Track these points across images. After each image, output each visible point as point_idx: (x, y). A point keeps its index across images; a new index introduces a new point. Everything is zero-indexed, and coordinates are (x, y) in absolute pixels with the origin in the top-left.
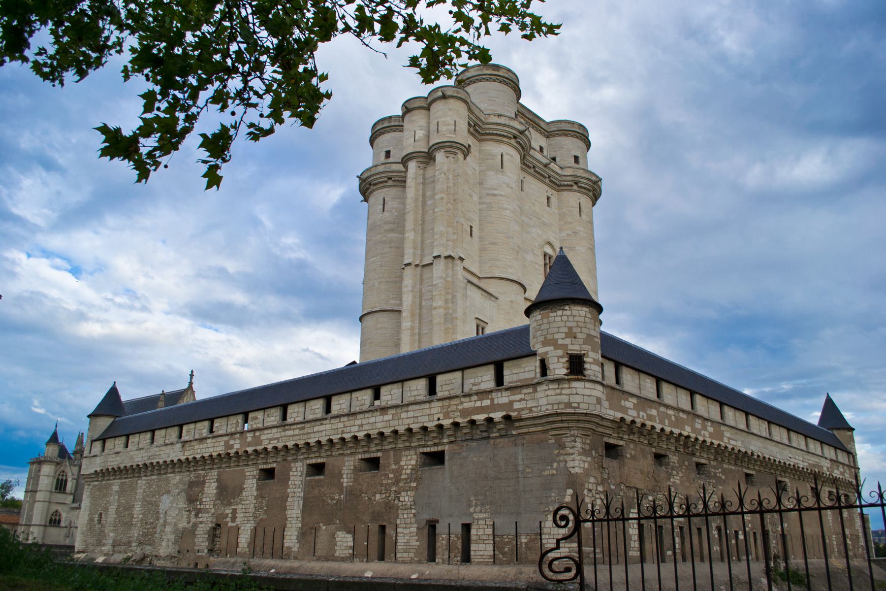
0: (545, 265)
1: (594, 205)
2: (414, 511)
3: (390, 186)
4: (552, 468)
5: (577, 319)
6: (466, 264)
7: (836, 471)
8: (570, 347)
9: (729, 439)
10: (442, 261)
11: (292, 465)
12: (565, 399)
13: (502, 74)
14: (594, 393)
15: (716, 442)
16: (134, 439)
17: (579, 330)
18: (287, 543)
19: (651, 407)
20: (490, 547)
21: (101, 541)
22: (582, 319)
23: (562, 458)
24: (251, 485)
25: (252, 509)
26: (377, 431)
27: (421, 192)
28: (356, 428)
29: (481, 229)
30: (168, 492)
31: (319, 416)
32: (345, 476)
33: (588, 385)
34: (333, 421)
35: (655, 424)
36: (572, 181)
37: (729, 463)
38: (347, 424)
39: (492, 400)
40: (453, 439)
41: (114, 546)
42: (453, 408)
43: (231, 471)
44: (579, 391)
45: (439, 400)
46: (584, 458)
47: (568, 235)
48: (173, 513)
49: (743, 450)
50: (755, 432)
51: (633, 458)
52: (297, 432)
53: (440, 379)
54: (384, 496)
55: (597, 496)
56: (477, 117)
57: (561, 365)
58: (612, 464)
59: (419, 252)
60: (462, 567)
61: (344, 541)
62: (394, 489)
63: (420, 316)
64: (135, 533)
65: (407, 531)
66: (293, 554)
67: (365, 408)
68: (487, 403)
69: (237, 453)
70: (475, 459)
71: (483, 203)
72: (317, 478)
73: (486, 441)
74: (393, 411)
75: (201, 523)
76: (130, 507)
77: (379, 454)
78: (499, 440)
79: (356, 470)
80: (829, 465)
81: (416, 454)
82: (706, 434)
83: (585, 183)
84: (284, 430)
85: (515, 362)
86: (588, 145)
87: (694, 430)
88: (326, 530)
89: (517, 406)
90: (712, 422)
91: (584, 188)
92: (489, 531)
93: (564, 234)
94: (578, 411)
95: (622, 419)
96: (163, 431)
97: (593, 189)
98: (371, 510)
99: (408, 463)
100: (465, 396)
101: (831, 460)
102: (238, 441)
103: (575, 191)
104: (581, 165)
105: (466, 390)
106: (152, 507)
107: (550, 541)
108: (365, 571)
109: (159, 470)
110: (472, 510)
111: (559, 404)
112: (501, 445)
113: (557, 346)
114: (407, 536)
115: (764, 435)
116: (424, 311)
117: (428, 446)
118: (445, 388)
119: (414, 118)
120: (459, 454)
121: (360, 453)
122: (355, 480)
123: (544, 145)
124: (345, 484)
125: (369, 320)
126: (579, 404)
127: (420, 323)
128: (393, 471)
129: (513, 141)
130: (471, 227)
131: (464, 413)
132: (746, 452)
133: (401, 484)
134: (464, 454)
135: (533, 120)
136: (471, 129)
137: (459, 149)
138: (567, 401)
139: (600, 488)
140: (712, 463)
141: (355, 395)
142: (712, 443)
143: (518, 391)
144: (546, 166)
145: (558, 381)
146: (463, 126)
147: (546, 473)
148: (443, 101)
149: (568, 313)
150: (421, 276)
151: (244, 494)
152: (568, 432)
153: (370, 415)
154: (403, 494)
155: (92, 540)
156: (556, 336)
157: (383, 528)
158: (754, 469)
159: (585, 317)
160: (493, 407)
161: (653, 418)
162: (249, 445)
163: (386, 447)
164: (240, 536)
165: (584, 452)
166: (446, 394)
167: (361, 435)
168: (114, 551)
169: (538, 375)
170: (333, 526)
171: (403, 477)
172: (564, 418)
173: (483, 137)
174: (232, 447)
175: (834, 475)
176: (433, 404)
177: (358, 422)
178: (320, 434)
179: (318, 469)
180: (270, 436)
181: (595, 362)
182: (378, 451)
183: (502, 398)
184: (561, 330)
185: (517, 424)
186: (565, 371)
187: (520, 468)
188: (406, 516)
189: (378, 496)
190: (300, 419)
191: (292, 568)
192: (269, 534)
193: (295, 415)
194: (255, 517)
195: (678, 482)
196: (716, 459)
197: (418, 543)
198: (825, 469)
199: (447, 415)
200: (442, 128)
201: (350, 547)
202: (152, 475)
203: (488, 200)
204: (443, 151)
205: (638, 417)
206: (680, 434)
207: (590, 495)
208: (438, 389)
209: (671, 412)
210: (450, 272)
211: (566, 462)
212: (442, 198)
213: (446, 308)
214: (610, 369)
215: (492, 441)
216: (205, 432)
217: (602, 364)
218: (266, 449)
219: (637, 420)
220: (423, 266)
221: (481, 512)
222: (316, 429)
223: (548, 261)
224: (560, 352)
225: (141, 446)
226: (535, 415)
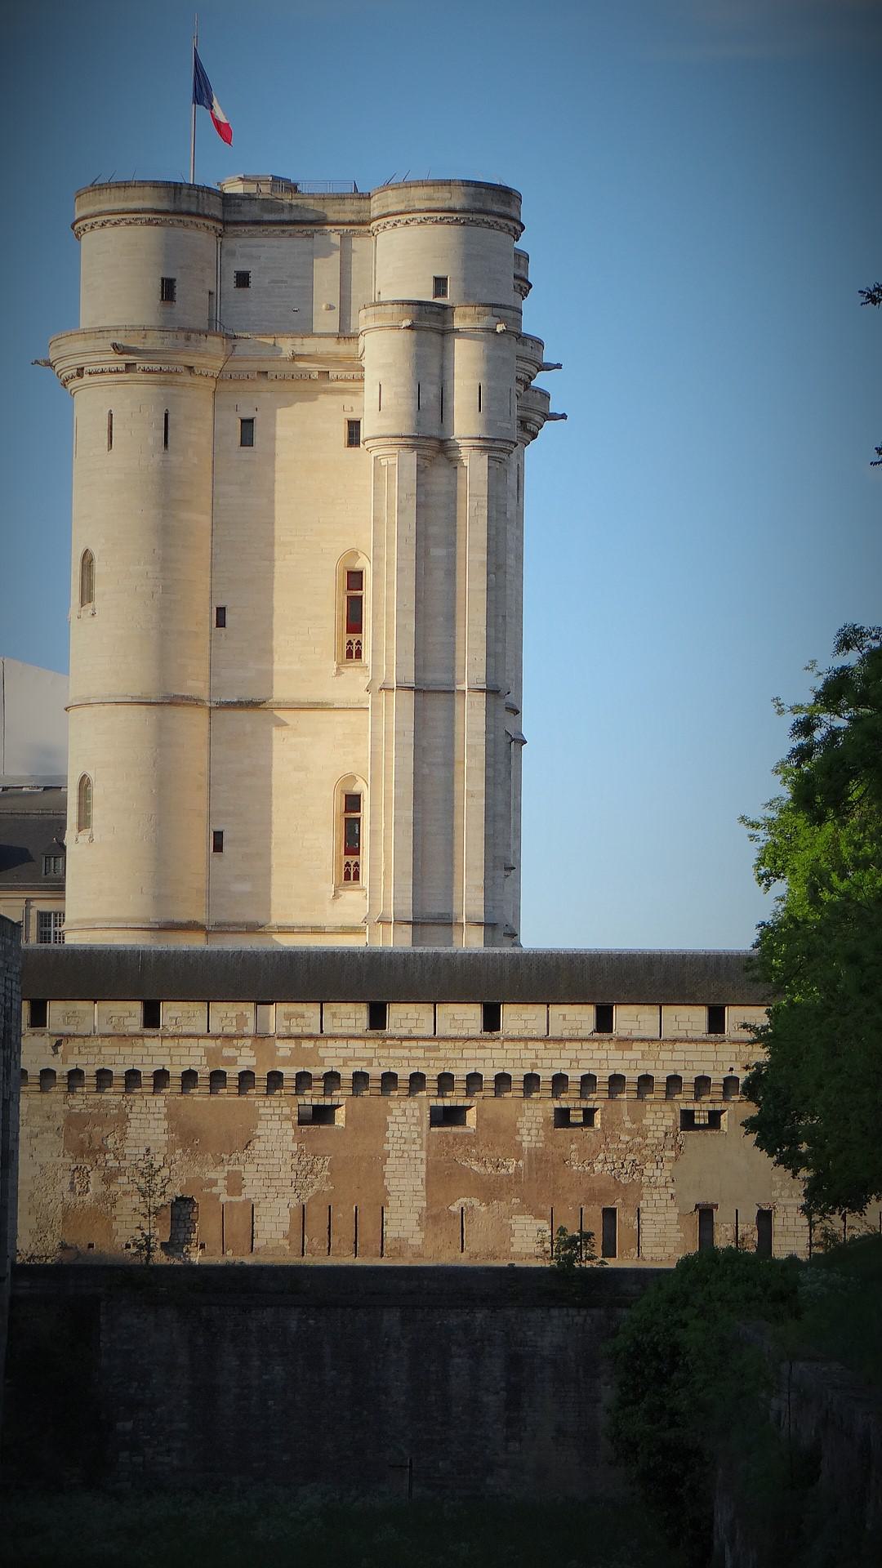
2: (671, 1191)
3: (184, 385)
11: (392, 1104)
18: (391, 1232)
32: (524, 1131)
34: (507, 1045)
38: (542, 1054)
52: (420, 1053)
54: (610, 1166)
62: (630, 1157)
74: (644, 1046)
81: (673, 1111)
99: (657, 1122)
110: (775, 1194)
151: (258, 1145)
157: (609, 1214)
167: (574, 1075)
171: (648, 1141)
176: (720, 1047)
222: (467, 1053)
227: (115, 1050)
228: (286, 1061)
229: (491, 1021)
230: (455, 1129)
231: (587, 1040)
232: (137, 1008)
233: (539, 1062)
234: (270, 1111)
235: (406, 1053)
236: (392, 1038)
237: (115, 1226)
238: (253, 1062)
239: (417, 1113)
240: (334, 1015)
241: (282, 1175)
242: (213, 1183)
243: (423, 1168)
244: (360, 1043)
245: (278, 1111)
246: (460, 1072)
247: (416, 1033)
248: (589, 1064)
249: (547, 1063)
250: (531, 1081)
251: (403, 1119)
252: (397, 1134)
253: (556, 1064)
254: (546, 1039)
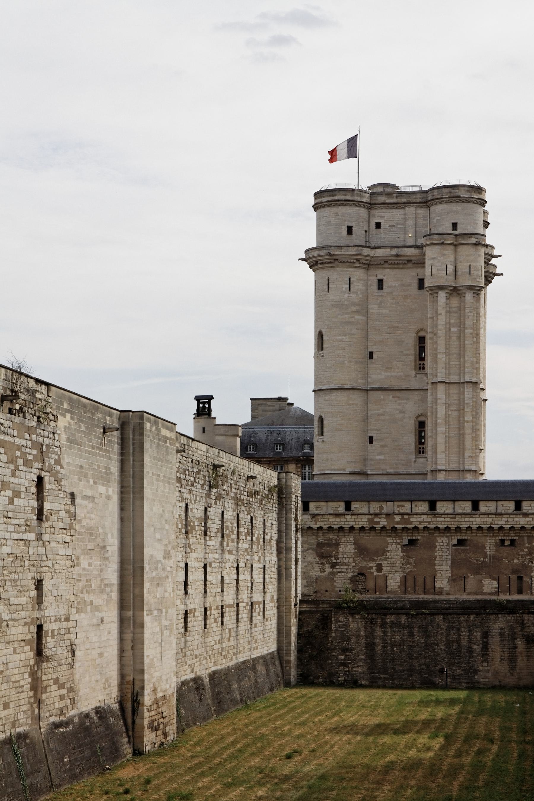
18: (438, 585)
26: (520, 526)
28: (504, 523)
34: (481, 516)
38: (495, 519)
52: (448, 519)
54: (521, 561)
62: (528, 557)
66: (445, 592)
67: (510, 512)
88: (474, 578)
98: (510, 568)
122: (497, 551)
124: (488, 553)
128: (527, 548)
141: (500, 503)
153: (515, 516)
157: (520, 578)
163: (522, 535)
170: (481, 576)
178: (471, 523)
189: (516, 561)
201: (496, 588)
222: (466, 519)
227: (334, 520)
228: (398, 523)
229: (475, 507)
230: (462, 548)
231: (511, 514)
232: (342, 504)
233: (493, 522)
234: (392, 541)
235: (443, 519)
236: (438, 514)
237: (335, 584)
238: (386, 523)
239: (447, 542)
240: (416, 506)
241: (397, 565)
242: (372, 568)
243: (450, 562)
244: (426, 516)
245: (395, 541)
246: (464, 526)
247: (447, 512)
248: (512, 523)
249: (496, 522)
250: (490, 529)
251: (442, 544)
252: (440, 549)
253: (500, 523)
254: (496, 514)
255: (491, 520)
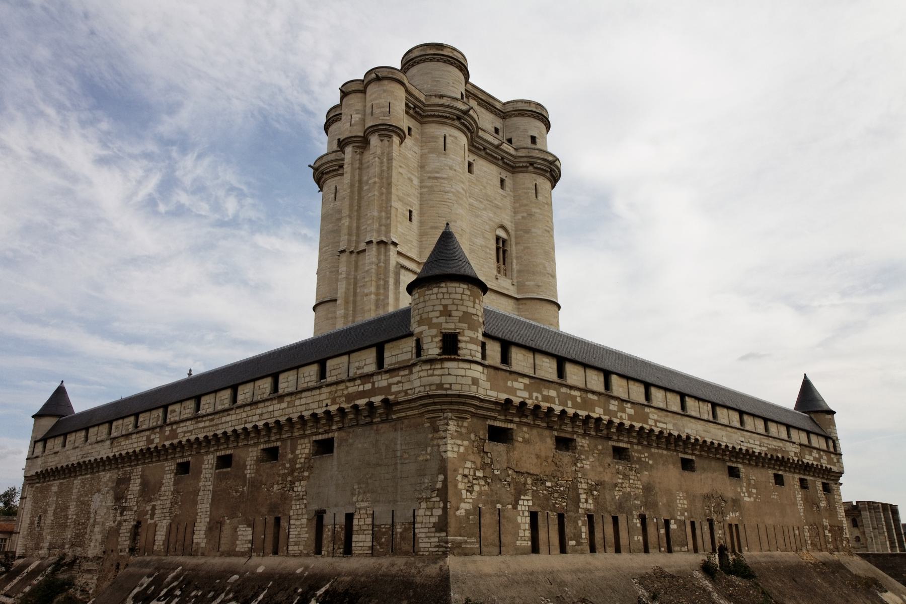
0: (498, 249)
1: (553, 187)
2: (305, 501)
4: (426, 453)
5: (453, 296)
6: (399, 249)
7: (807, 457)
8: (445, 326)
9: (656, 421)
10: (374, 248)
11: (205, 457)
12: (437, 380)
13: (446, 54)
14: (469, 373)
15: (637, 425)
16: (71, 438)
17: (455, 307)
19: (549, 389)
20: (369, 538)
21: (38, 545)
22: (459, 296)
23: (435, 442)
24: (169, 479)
25: (168, 506)
27: (357, 178)
29: (421, 214)
30: (99, 491)
31: (227, 406)
33: (462, 365)
35: (553, 406)
36: (528, 162)
37: (658, 447)
39: (373, 383)
40: (340, 425)
41: (49, 549)
42: (339, 393)
43: (152, 468)
44: (453, 372)
45: (327, 385)
46: (459, 442)
47: (523, 217)
48: (102, 512)
49: (676, 433)
50: (693, 414)
51: (526, 442)
52: (207, 423)
53: (330, 364)
54: (280, 486)
55: (475, 482)
56: (416, 99)
57: (434, 345)
58: (498, 449)
59: (354, 238)
60: (344, 560)
61: (245, 534)
62: (289, 479)
63: (355, 302)
64: (69, 534)
65: (298, 523)
66: (200, 550)
67: (266, 396)
68: (368, 386)
69: (156, 447)
70: (360, 446)
71: (425, 187)
72: (225, 470)
73: (368, 428)
75: (125, 521)
76: (66, 508)
77: (279, 444)
78: (380, 425)
79: (259, 461)
80: (798, 450)
82: (625, 416)
83: (541, 164)
84: (197, 422)
85: (395, 343)
86: (548, 126)
87: (607, 411)
89: (394, 389)
90: (633, 403)
91: (540, 169)
92: (369, 521)
93: (519, 216)
94: (449, 392)
95: (508, 401)
96: (96, 429)
97: (551, 171)
100: (350, 380)
101: (801, 445)
102: (158, 435)
103: (531, 172)
104: (538, 146)
105: (351, 374)
106: (84, 506)
107: (422, 530)
108: (258, 566)
109: (92, 468)
110: (355, 499)
111: (430, 385)
112: (382, 431)
113: (431, 325)
114: (299, 529)
115: (705, 417)
116: (359, 298)
117: (320, 434)
118: (334, 373)
119: (351, 102)
120: (346, 440)
121: (262, 443)
122: (257, 471)
123: (499, 126)
124: (248, 476)
125: (319, 308)
126: (451, 384)
127: (354, 310)
129: (457, 123)
130: (411, 212)
131: (350, 398)
132: (679, 436)
133: (296, 474)
134: (351, 441)
135: (487, 102)
136: (411, 112)
137: (393, 131)
138: (438, 382)
139: (480, 474)
140: (635, 447)
142: (632, 426)
143: (396, 373)
144: (498, 147)
145: (431, 361)
146: (399, 107)
147: (421, 458)
148: (378, 83)
149: (444, 290)
150: (356, 262)
151: (163, 489)
152: (441, 414)
154: (297, 484)
155: (31, 544)
156: (431, 315)
157: (278, 520)
158: (693, 454)
159: (463, 294)
160: (374, 392)
161: (553, 400)
162: (167, 439)
164: (158, 533)
165: (460, 436)
166: (334, 379)
168: (49, 555)
169: (414, 356)
170: (236, 520)
171: (298, 466)
172: (436, 400)
173: (425, 120)
174: (152, 441)
175: (805, 461)
177: (259, 411)
179: (225, 462)
180: (184, 429)
181: (472, 341)
182: (277, 440)
183: (382, 381)
184: (436, 308)
185: (395, 408)
186: (438, 351)
187: (399, 454)
188: (298, 507)
190: (210, 411)
191: (197, 565)
192: (182, 530)
193: (206, 406)
194: (171, 513)
195: (588, 467)
196: (639, 443)
197: (307, 535)
198: (792, 454)
199: (334, 402)
200: (377, 111)
202: (86, 474)
203: (429, 183)
204: (377, 134)
205: (531, 398)
206: (588, 417)
207: (466, 480)
208: (328, 374)
209: (577, 393)
210: (382, 257)
211: (439, 446)
212: (375, 183)
213: (377, 294)
214: (494, 350)
215: (375, 427)
216: (131, 428)
217: (483, 345)
218: (180, 442)
219: (529, 402)
220: (359, 253)
221: (362, 501)
222: (223, 420)
223: (501, 245)
224: (434, 332)
225: (76, 445)
226: (410, 397)
254: (251, 404)
255: (244, 415)
